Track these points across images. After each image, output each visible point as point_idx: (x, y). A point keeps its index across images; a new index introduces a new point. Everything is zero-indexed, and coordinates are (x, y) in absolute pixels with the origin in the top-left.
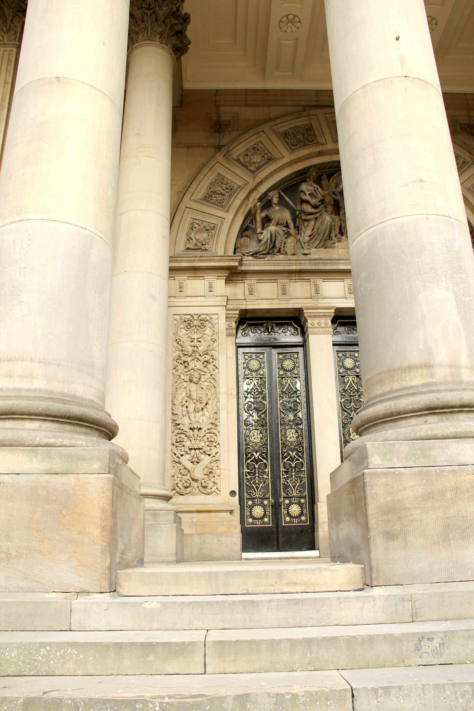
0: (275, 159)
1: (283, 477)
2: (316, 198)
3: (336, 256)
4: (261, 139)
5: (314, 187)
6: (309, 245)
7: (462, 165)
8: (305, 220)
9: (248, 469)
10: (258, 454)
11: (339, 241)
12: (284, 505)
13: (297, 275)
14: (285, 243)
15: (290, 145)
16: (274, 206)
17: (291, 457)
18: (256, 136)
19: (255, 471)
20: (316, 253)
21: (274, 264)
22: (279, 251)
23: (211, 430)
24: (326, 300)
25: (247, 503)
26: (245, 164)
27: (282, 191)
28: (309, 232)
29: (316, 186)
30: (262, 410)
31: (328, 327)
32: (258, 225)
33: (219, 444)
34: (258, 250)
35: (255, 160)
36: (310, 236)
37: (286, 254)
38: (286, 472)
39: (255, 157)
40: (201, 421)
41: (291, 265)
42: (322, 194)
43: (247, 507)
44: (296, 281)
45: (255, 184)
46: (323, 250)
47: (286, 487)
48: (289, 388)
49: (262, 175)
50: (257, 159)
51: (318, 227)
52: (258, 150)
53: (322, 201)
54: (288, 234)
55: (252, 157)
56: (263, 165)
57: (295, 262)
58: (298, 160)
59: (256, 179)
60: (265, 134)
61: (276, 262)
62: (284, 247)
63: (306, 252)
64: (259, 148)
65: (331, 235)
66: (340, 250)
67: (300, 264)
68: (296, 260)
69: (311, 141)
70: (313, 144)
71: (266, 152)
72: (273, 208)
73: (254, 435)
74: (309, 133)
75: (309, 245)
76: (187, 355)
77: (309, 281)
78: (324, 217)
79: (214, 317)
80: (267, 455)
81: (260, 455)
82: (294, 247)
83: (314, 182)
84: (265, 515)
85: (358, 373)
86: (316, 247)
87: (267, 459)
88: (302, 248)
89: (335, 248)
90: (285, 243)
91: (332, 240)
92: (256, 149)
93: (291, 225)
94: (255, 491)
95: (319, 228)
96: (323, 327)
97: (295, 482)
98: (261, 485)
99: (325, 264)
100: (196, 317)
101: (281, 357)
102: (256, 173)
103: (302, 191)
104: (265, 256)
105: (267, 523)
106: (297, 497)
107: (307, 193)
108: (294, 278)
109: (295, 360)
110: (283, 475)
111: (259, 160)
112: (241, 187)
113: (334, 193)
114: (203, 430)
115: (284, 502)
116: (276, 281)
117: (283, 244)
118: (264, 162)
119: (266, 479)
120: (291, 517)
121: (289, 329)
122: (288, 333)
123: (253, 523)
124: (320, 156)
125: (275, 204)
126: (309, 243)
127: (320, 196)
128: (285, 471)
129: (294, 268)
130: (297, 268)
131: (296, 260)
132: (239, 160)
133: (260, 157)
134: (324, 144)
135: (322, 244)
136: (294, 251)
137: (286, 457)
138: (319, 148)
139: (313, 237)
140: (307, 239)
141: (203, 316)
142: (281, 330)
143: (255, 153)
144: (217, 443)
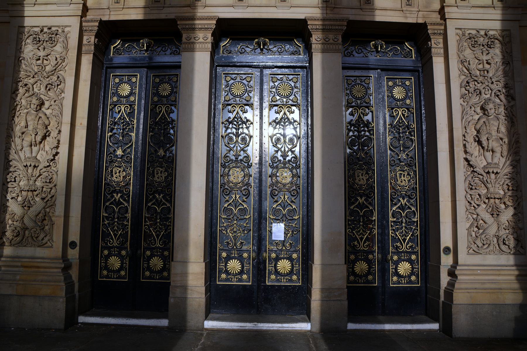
1: (146, 225)
9: (106, 213)
10: (119, 195)
12: (144, 257)
17: (157, 200)
19: (114, 216)
23: (49, 168)
24: (208, 9)
25: (102, 252)
30: (127, 144)
31: (206, 43)
33: (55, 186)
38: (150, 219)
40: (38, 157)
43: (102, 257)
47: (148, 236)
48: (163, 118)
73: (116, 173)
76: (30, 76)
79: (66, 29)
80: (129, 197)
81: (121, 196)
84: (121, 268)
85: (247, 101)
87: (128, 202)
94: (113, 240)
96: (201, 43)
97: (159, 231)
98: (120, 232)
100: (46, 30)
101: (157, 80)
105: (124, 277)
106: (160, 249)
109: (173, 84)
110: (145, 221)
114: (39, 169)
115: (144, 253)
119: (126, 225)
120: (151, 271)
121: (170, 47)
122: (169, 51)
123: (107, 277)
128: (148, 217)
137: (151, 200)
141: (53, 29)
142: (160, 49)
144: (53, 185)
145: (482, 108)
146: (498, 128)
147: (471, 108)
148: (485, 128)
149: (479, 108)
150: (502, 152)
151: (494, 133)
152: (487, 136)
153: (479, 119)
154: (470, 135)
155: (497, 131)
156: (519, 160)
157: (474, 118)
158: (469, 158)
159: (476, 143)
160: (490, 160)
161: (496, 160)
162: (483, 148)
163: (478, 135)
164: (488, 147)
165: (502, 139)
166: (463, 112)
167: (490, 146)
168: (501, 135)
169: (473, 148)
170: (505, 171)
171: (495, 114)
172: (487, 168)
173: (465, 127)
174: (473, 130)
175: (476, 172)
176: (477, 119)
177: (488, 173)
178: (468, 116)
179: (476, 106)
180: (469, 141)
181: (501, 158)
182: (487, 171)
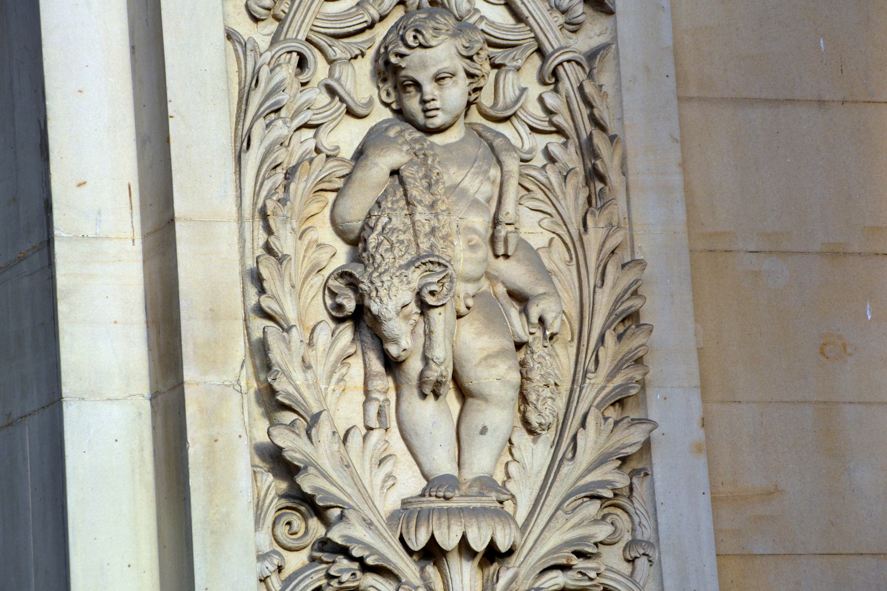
145: (388, 72)
146: (496, 222)
147: (302, 63)
148: (399, 221)
149: (365, 66)
150: (523, 398)
151: (466, 257)
152: (415, 277)
153: (360, 154)
154: (296, 269)
155: (493, 240)
156: (647, 446)
157: (328, 140)
158: (293, 445)
159: (346, 332)
160: (442, 462)
161: (482, 460)
162: (392, 365)
163: (357, 271)
164: (426, 360)
165: (520, 298)
166: (244, 100)
167: (440, 352)
168: (515, 272)
169: (321, 369)
170: (553, 540)
171: (475, 116)
172: (424, 516)
173: (264, 216)
174: (325, 233)
175: (344, 551)
176: (348, 152)
177: (432, 553)
178: (280, 129)
179: (338, 50)
180: (292, 315)
181: (522, 438)
182: (419, 541)
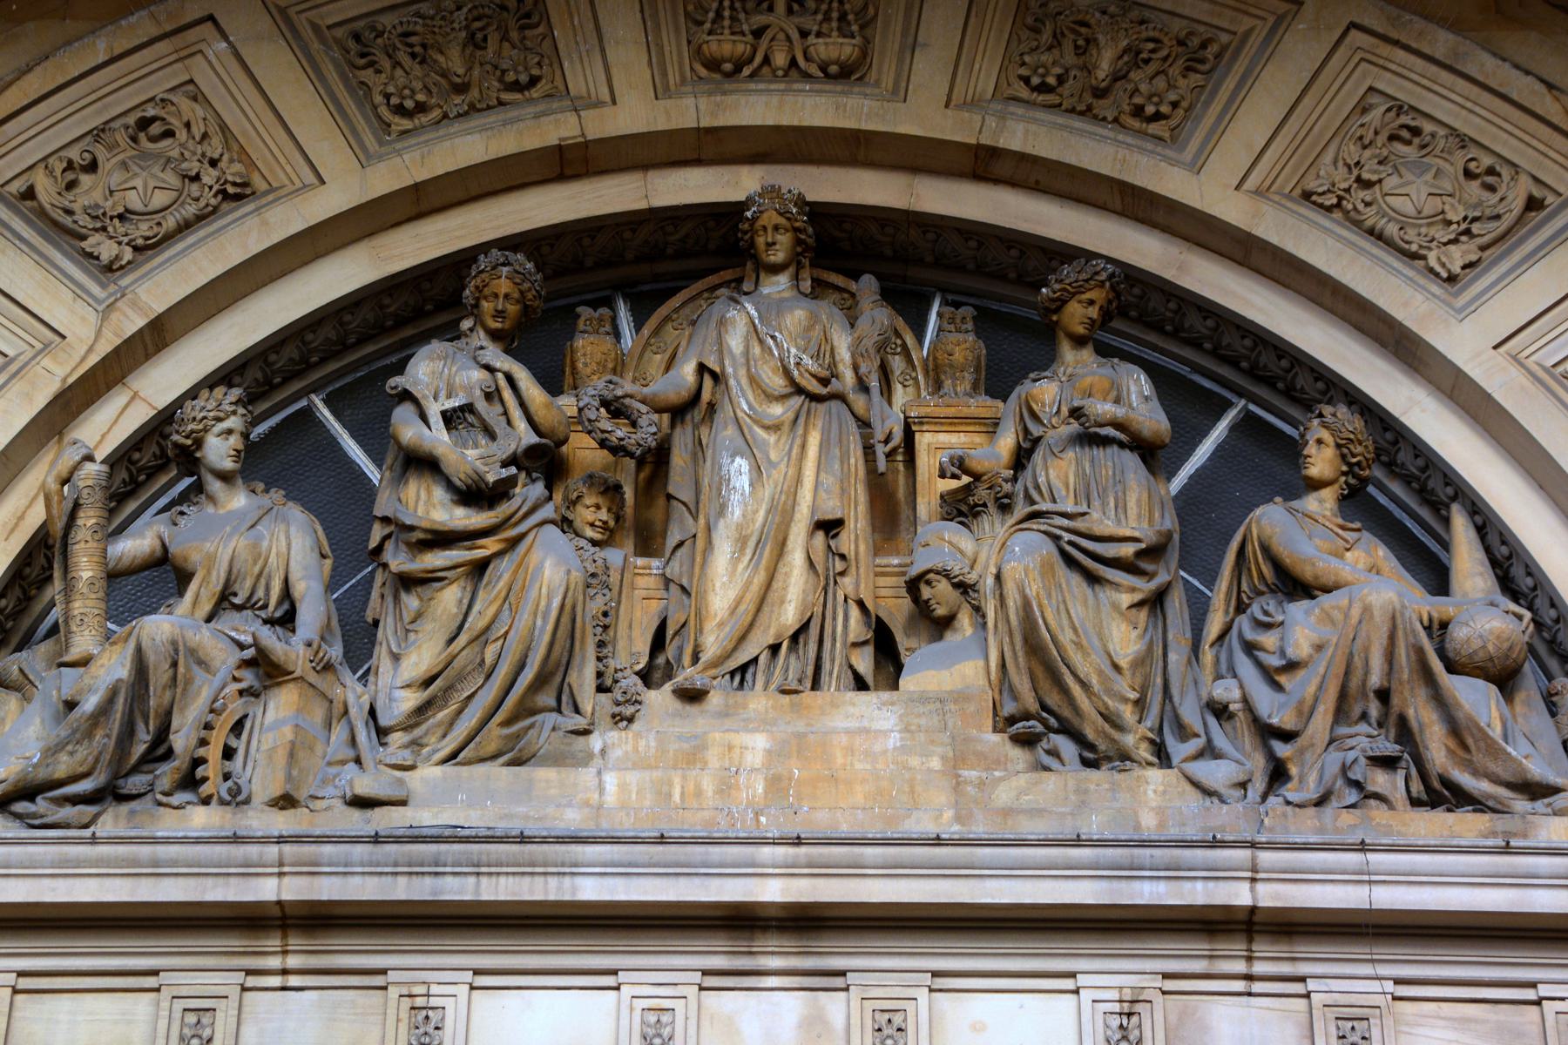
0: (272, 190)
2: (492, 436)
3: (572, 819)
4: (199, 71)
5: (489, 368)
6: (416, 744)
7: (1519, 221)
8: (408, 582)
11: (622, 720)
13: (295, 942)
14: (238, 728)
15: (384, 111)
16: (215, 486)
18: (162, 47)
20: (442, 795)
21: (135, 862)
22: (190, 781)
26: (67, 221)
27: (327, 402)
28: (422, 657)
29: (504, 362)
32: (78, 606)
34: (43, 775)
35: (134, 201)
36: (428, 682)
37: (237, 798)
39: (138, 183)
41: (249, 870)
42: (541, 415)
44: (294, 981)
45: (104, 348)
46: (497, 773)
49: (163, 286)
50: (146, 187)
51: (482, 624)
52: (169, 134)
53: (545, 461)
54: (265, 670)
55: (116, 179)
56: (185, 227)
57: (273, 851)
58: (419, 202)
59: (114, 316)
60: (225, 37)
61: (145, 851)
62: (228, 753)
63: (365, 785)
64: (176, 123)
65: (573, 677)
66: (611, 780)
67: (312, 870)
68: (281, 840)
69: (516, 87)
70: (531, 100)
71: (215, 148)
72: (212, 499)
74: (514, 35)
75: (416, 744)
77: (378, 980)
78: (534, 558)
82: (292, 755)
83: (495, 336)
86: (453, 756)
88: (358, 761)
89: (586, 759)
90: (238, 728)
91: (577, 710)
92: (156, 129)
93: (311, 615)
95: (488, 628)
99: (478, 869)
102: (124, 282)
103: (406, 396)
104: (91, 810)
107: (434, 410)
108: (274, 962)
111: (160, 199)
112: (13, 368)
113: (616, 409)
116: (150, 982)
117: (218, 739)
118: (191, 210)
124: (576, 176)
125: (225, 477)
126: (417, 732)
127: (521, 425)
129: (266, 890)
130: (286, 896)
131: (281, 840)
132: (29, 194)
133: (173, 180)
134: (599, 104)
135: (495, 735)
136: (289, 778)
138: (557, 129)
139: (449, 689)
140: (408, 700)
143: (144, 155)
